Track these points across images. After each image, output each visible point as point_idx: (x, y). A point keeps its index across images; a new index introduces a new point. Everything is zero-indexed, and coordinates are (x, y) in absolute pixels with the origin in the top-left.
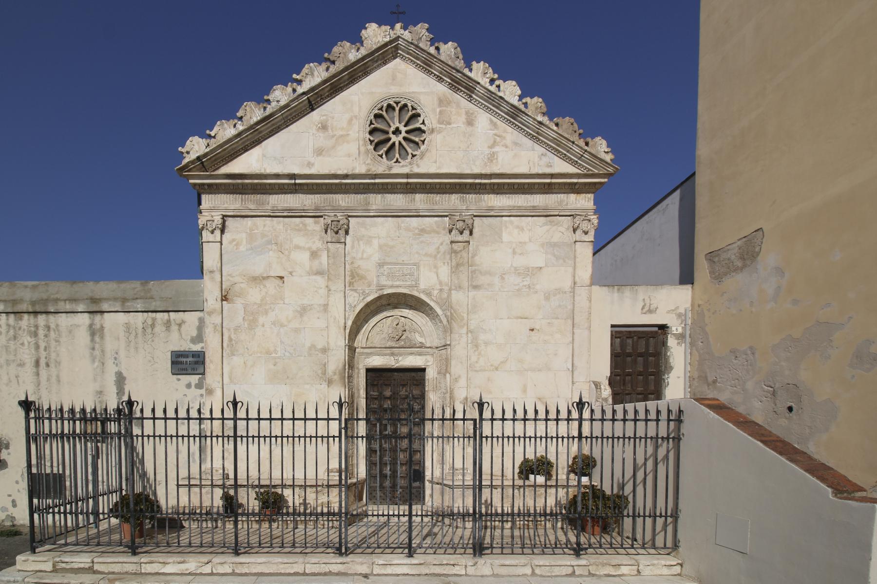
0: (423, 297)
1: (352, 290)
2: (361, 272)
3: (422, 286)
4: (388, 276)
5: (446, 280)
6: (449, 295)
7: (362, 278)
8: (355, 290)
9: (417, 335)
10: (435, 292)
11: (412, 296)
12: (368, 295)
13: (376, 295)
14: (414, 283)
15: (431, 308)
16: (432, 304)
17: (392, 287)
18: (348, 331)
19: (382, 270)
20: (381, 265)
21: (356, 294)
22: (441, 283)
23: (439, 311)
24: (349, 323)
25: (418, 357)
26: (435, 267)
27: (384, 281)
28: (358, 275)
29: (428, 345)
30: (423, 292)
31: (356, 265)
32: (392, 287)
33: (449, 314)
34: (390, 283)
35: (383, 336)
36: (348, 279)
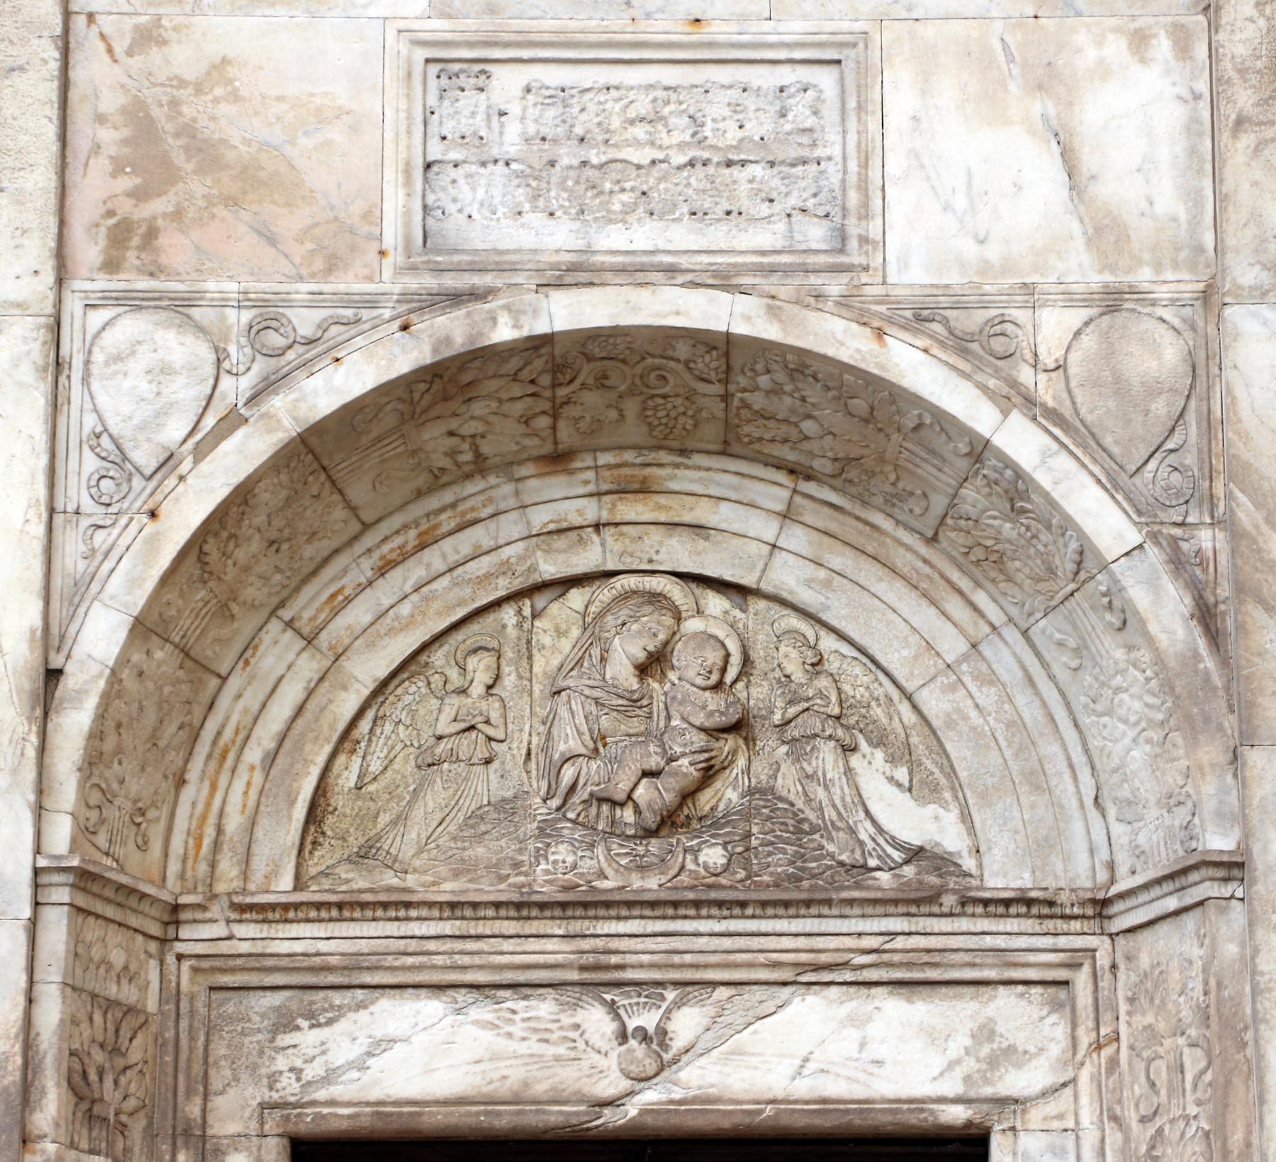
0: (914, 367)
1: (132, 302)
2: (236, 128)
3: (917, 248)
4: (534, 175)
5: (1169, 201)
6: (1204, 367)
7: (253, 183)
8: (180, 307)
9: (874, 774)
10: (1053, 328)
11: (801, 365)
12: (319, 349)
13: (401, 357)
14: (815, 234)
15: (1016, 490)
16: (1021, 442)
17: (576, 273)
18: (75, 722)
19: (465, 111)
20: (455, 65)
21: (180, 348)
22: (1105, 233)
23: (1105, 522)
24: (101, 637)
25: (893, 1011)
26: (1047, 78)
27: (495, 218)
28: (208, 154)
29: (1002, 874)
30: (921, 317)
31: (182, 59)
32: (576, 273)
33: (1206, 539)
34: (557, 237)
35: (488, 786)
36: (96, 188)
